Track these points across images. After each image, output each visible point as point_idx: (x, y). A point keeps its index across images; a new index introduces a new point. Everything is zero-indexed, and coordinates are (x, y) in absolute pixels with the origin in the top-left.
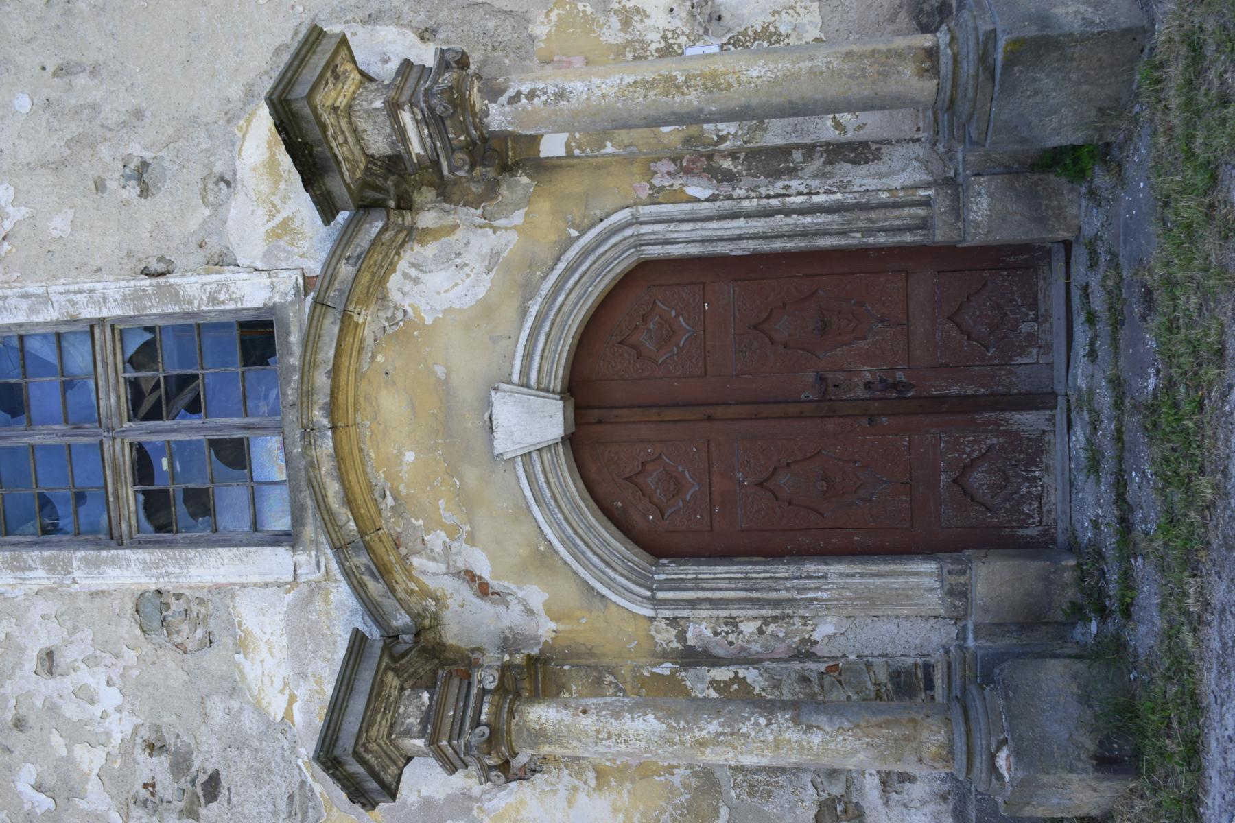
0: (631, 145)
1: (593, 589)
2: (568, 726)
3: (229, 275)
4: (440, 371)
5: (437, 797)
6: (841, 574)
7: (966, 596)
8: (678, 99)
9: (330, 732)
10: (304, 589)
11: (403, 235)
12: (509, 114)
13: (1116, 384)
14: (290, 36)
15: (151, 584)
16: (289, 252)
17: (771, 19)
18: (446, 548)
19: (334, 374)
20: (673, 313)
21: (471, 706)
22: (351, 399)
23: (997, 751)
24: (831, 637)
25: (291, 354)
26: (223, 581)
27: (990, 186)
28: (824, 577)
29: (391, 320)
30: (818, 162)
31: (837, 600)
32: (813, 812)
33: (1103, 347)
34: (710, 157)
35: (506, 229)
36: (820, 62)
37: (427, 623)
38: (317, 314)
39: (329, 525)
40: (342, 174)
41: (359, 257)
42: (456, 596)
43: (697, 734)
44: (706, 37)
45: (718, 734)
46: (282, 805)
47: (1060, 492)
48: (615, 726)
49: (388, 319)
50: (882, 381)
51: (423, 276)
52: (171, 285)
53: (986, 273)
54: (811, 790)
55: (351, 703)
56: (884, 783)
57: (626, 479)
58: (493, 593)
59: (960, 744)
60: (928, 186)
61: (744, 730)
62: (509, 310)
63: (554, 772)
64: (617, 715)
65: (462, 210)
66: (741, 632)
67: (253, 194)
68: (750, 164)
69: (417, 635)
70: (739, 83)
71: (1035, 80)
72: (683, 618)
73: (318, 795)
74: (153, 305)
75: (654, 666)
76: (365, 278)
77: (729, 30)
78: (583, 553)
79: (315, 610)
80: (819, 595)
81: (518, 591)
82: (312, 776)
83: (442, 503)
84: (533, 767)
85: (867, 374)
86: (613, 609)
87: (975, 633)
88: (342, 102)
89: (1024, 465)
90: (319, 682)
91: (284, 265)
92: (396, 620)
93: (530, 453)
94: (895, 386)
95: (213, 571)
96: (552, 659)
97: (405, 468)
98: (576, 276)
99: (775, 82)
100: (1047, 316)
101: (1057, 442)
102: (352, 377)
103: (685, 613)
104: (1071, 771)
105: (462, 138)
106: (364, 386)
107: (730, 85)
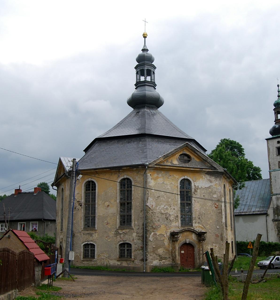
15: (179, 217)
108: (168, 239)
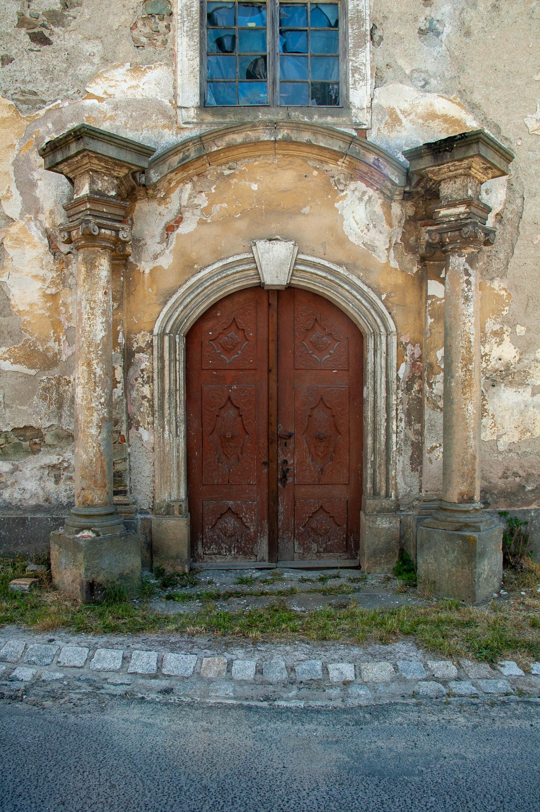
0: (431, 333)
1: (171, 297)
2: (97, 283)
3: (369, 82)
4: (306, 210)
5: (37, 192)
6: (179, 445)
7: (167, 514)
8: (460, 365)
9: (98, 135)
10: (172, 113)
11: (388, 193)
12: (459, 268)
13: (292, 592)
14: (505, 135)
16: (381, 121)
17: (490, 413)
18: (196, 206)
19: (309, 144)
20: (332, 352)
21: (109, 223)
22: (291, 153)
23: (92, 531)
24: (141, 438)
25: (320, 116)
26: (178, 59)
27: (394, 528)
28: (177, 435)
29: (338, 182)
30: (413, 438)
31: (163, 443)
32: (34, 425)
33: (308, 586)
34: (421, 377)
35: (388, 257)
36: (472, 442)
37: (150, 192)
38: (346, 137)
39: (216, 134)
40: (432, 166)
41: (378, 166)
42: (166, 211)
43: (95, 361)
44: (484, 378)
45: (95, 374)
46: (30, 87)
47: (223, 564)
48: (98, 312)
49: (339, 179)
50: (288, 469)
51: (363, 204)
52: (365, 43)
53: (345, 526)
54: (48, 424)
55: (113, 147)
56: (54, 466)
57: (234, 319)
58: (167, 234)
59: (94, 511)
60: (396, 497)
61: (97, 389)
62: (341, 255)
63: (55, 268)
64: (104, 313)
65: (400, 231)
66: (143, 386)
67: (417, 102)
68: (415, 400)
69: (144, 186)
70: (465, 399)
71: (454, 551)
72: (152, 351)
73: (37, 113)
74: (354, 30)
75: (123, 332)
76: (365, 169)
77: (487, 391)
78: (192, 292)
79: (158, 119)
80: (167, 432)
81: (169, 251)
82: (50, 109)
83: (225, 205)
84: (57, 254)
85: (292, 462)
86: (158, 309)
87: (145, 519)
88: (473, 172)
89: (238, 546)
90: (112, 118)
91: (374, 118)
92: (154, 173)
93: (255, 262)
94: (285, 477)
95: (185, 53)
96: (126, 269)
97: (247, 183)
98: (359, 297)
99: (464, 418)
100: (320, 558)
101: (250, 563)
102: (305, 154)
103: (155, 353)
104: (86, 570)
105: (447, 240)
106: (299, 161)
107: (464, 394)
108: (46, 241)
